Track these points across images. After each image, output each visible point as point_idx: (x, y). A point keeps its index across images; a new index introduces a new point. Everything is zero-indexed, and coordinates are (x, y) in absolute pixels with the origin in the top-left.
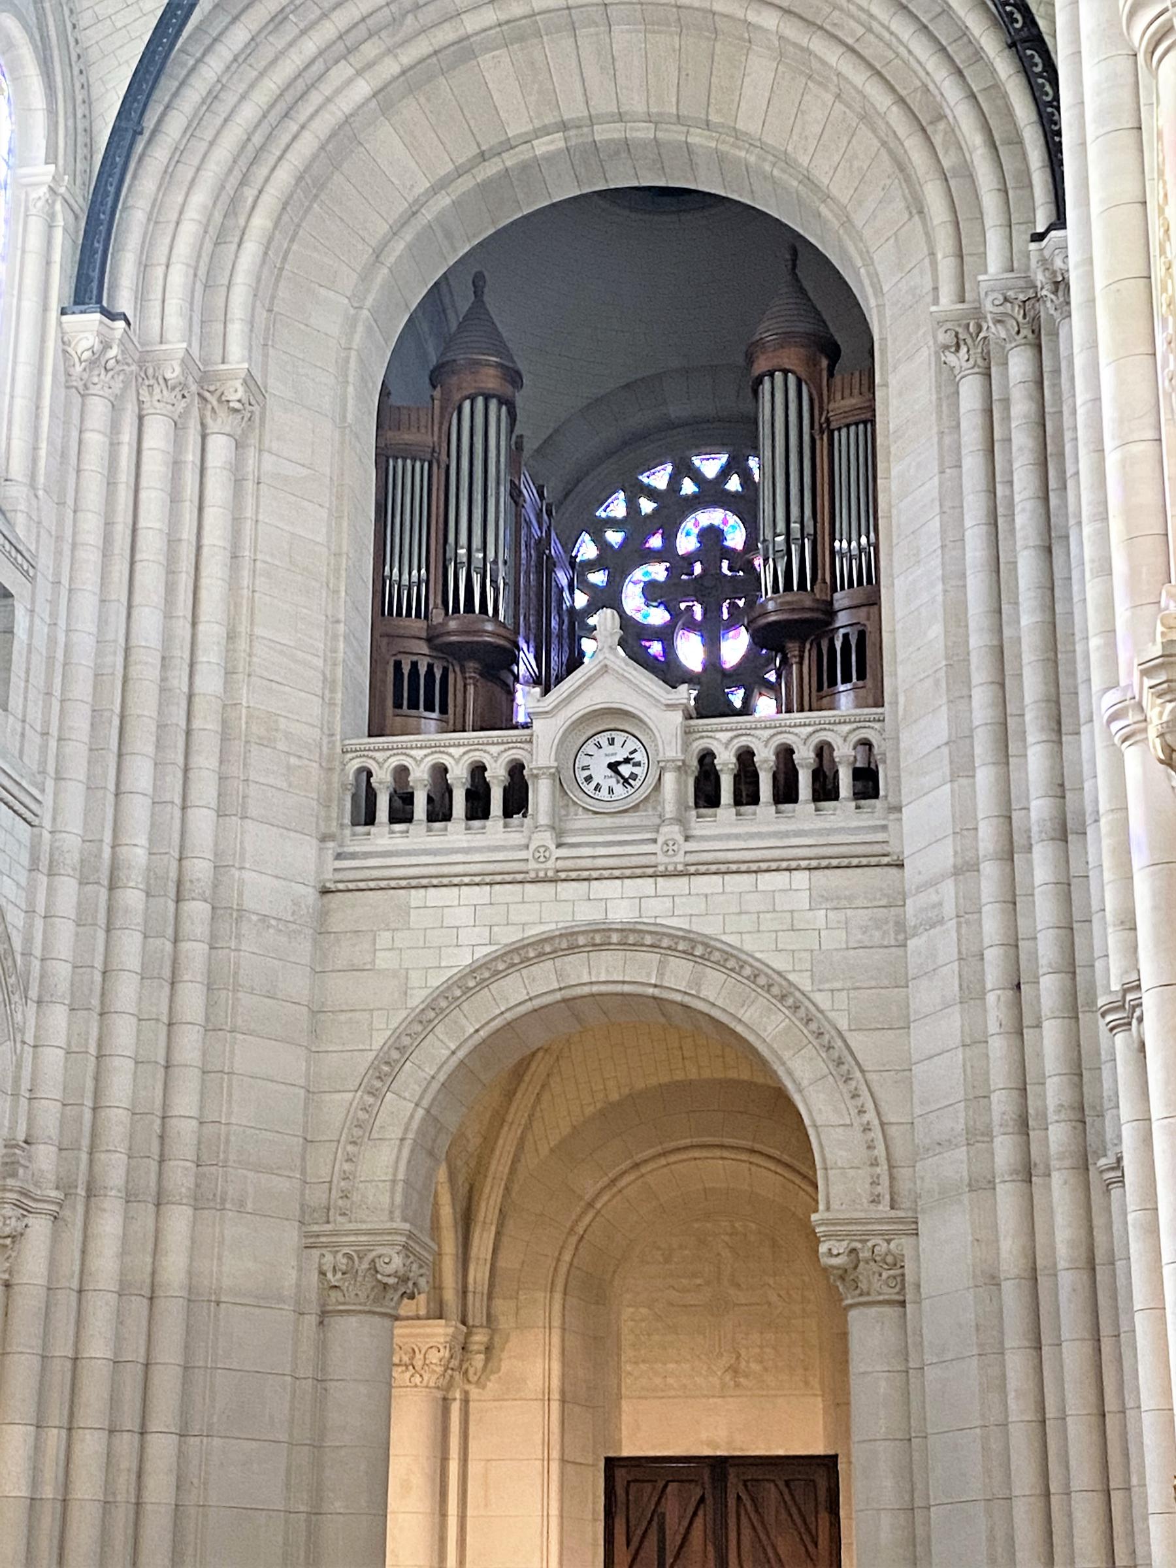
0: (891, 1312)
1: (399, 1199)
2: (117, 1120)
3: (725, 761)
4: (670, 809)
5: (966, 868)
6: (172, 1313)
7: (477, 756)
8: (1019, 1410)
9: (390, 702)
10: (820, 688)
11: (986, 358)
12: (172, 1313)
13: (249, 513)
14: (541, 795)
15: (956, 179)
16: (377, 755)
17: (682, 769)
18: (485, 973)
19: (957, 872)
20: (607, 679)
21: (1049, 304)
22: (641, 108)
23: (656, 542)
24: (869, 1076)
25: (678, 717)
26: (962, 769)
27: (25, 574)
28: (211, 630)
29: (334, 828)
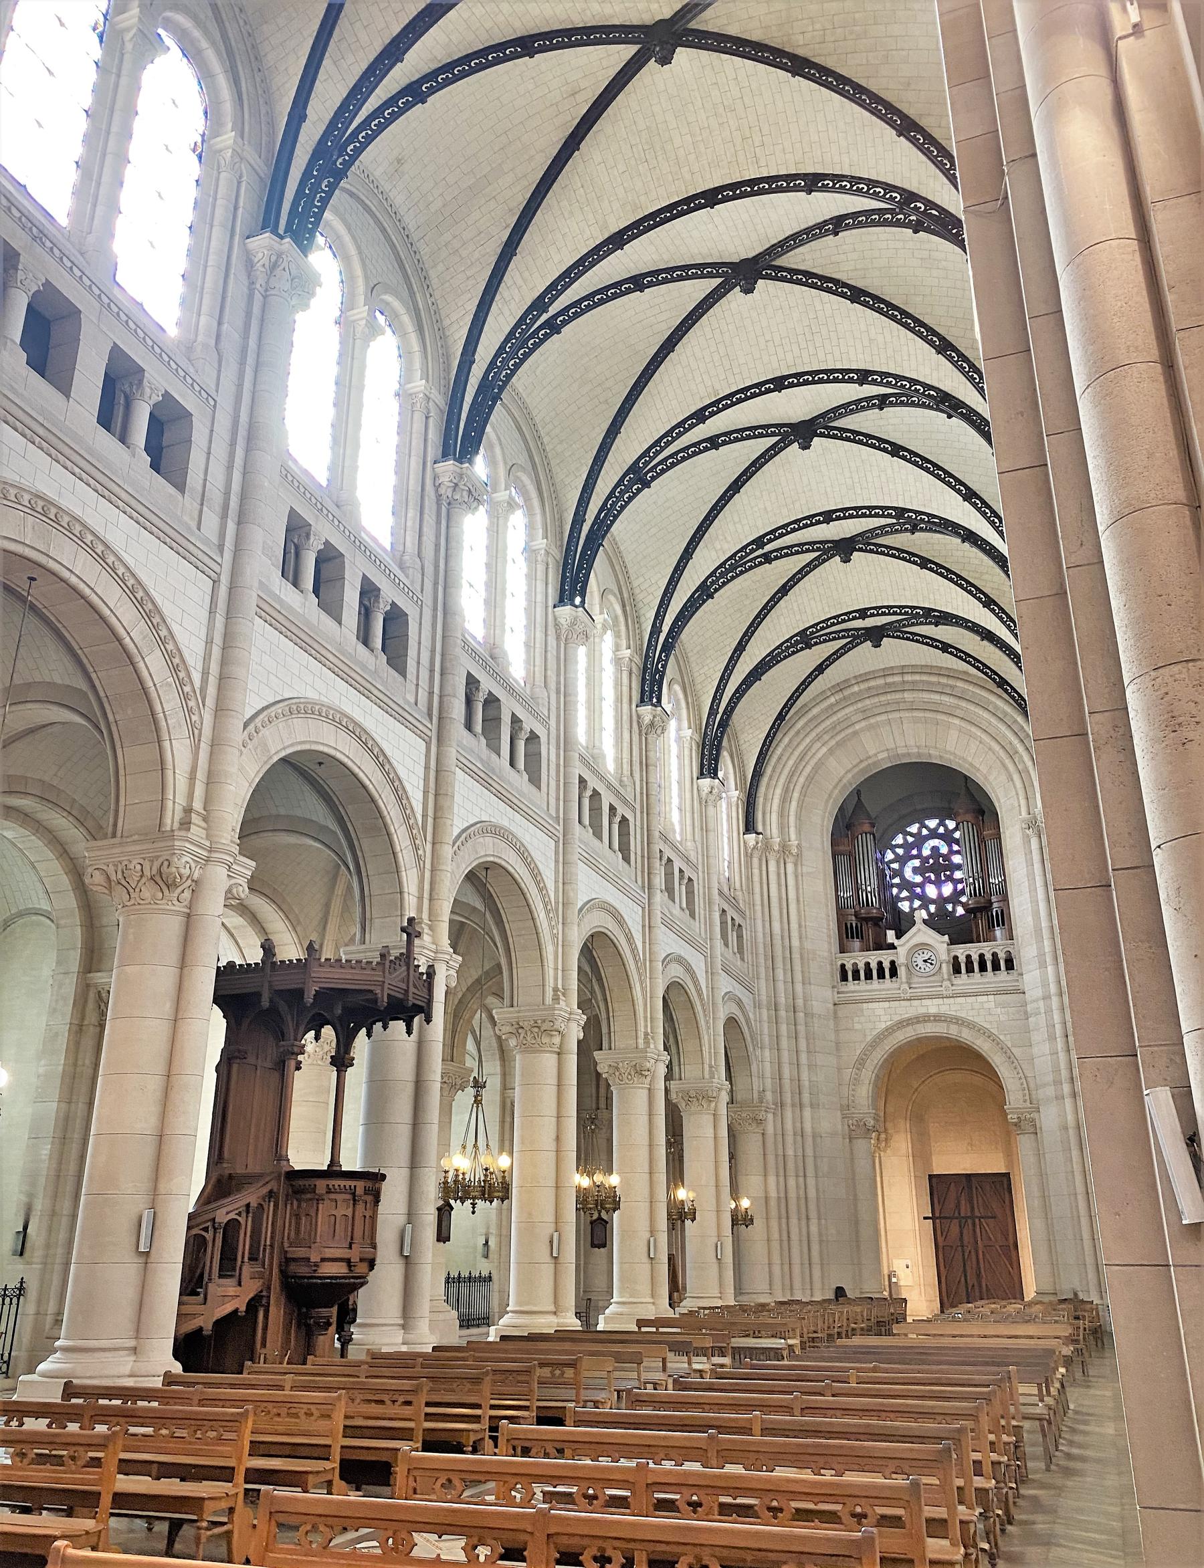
0: (1032, 1136)
3: (962, 959)
4: (946, 977)
5: (1047, 997)
6: (809, 1141)
8: (1077, 1168)
12: (809, 1141)
14: (902, 971)
18: (890, 1031)
23: (914, 852)
26: (1043, 965)
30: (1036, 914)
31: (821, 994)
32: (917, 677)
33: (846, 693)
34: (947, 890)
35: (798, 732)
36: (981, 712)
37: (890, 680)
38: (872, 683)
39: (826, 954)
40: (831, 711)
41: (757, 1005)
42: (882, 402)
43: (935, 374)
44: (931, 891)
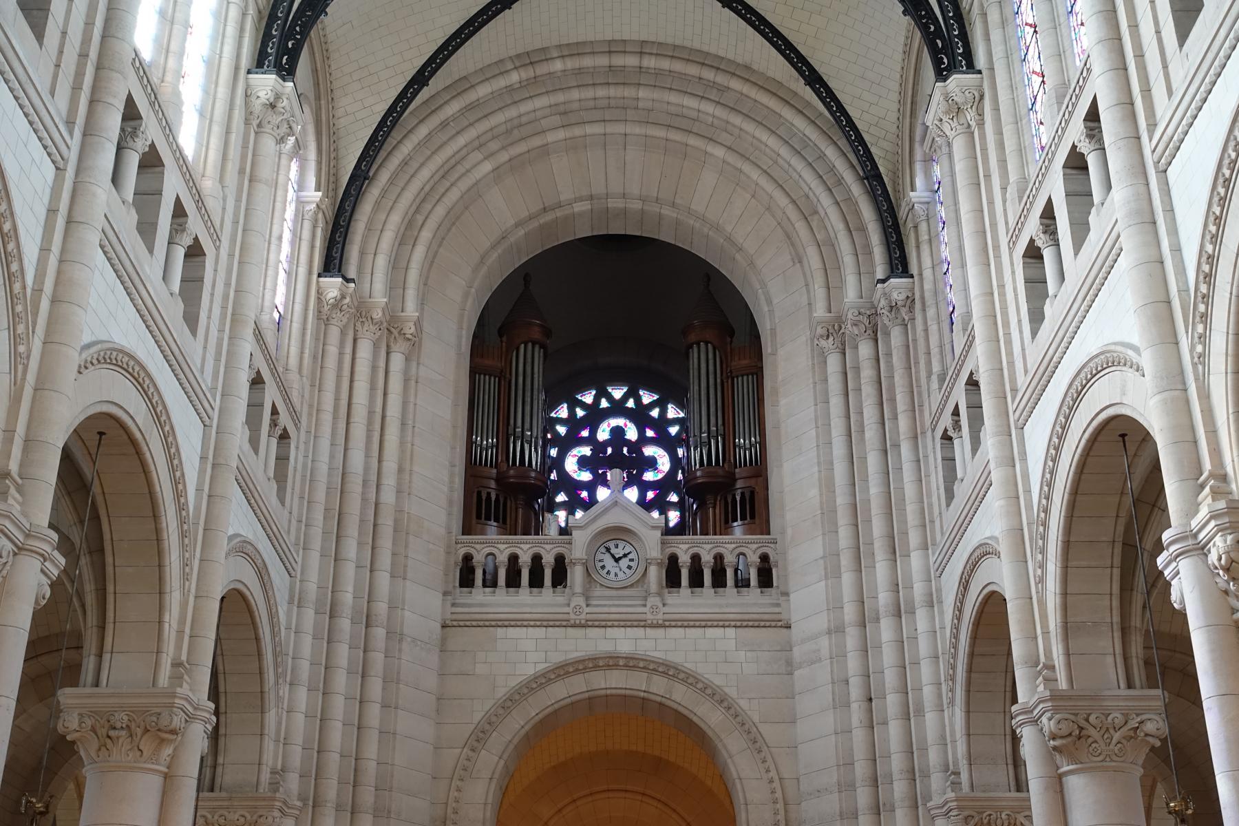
1: (488, 814)
2: (333, 760)
3: (684, 559)
5: (837, 630)
7: (536, 550)
9: (474, 516)
10: (727, 522)
11: (843, 344)
13: (412, 399)
14: (576, 575)
15: (826, 247)
16: (477, 546)
17: (660, 564)
19: (829, 632)
20: (616, 510)
21: (884, 318)
22: (636, 192)
23: (585, 433)
24: (773, 750)
25: (658, 533)
26: (833, 573)
27: (296, 425)
28: (390, 465)
29: (450, 588)
30: (828, 485)
31: (423, 600)
32: (665, 64)
33: (542, 69)
35: (444, 125)
36: (764, 136)
37: (618, 61)
38: (587, 62)
39: (443, 531)
40: (511, 96)
41: (297, 600)
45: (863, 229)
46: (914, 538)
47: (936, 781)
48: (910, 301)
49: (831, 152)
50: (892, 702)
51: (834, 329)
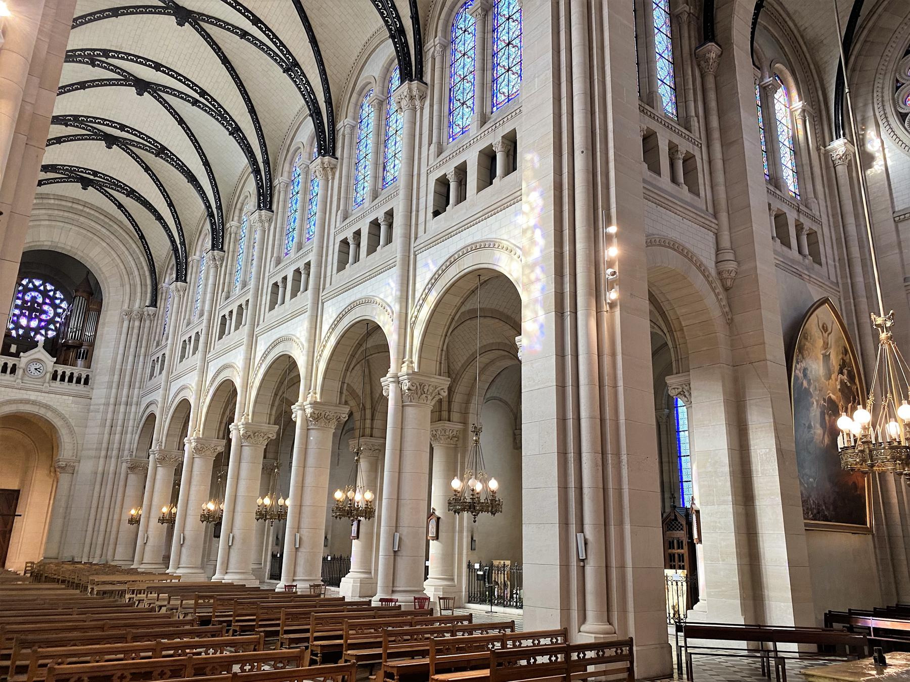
3: (60, 373)
14: (19, 372)
15: (133, 287)
23: (20, 295)
30: (115, 361)
32: (92, 212)
33: (45, 201)
34: (34, 324)
36: (121, 246)
37: (75, 206)
38: (64, 203)
42: (195, 102)
43: (239, 117)
44: (23, 321)
45: (146, 286)
46: (137, 385)
47: (126, 453)
48: (154, 315)
49: (142, 259)
50: (119, 429)
51: (129, 313)
